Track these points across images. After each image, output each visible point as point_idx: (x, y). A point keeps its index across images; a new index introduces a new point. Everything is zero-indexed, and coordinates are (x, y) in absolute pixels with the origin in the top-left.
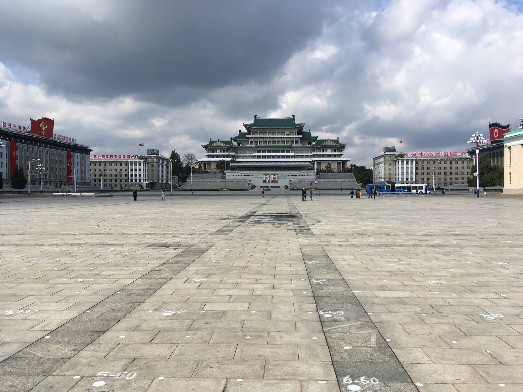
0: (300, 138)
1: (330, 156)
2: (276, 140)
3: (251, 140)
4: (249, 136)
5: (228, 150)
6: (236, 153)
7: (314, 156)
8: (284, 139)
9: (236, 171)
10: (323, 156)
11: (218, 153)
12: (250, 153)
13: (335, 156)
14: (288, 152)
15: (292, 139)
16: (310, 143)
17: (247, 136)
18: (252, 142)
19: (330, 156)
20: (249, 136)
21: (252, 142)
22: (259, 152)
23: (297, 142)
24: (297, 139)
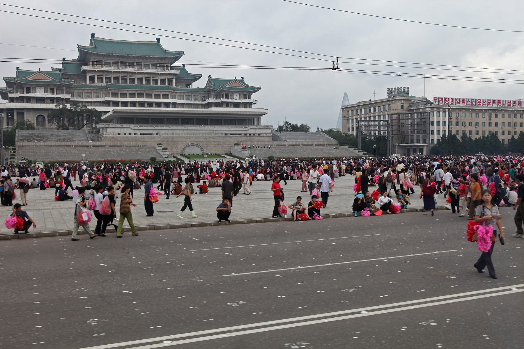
0: (176, 75)
1: (236, 105)
2: (136, 76)
3: (92, 75)
4: (88, 68)
5: (60, 88)
6: (73, 96)
7: (209, 105)
8: (148, 76)
9: (125, 126)
10: (227, 105)
11: (40, 93)
12: (97, 97)
13: (245, 105)
14: (166, 96)
15: (163, 77)
16: (188, 85)
17: (84, 68)
18: (92, 79)
19: (236, 105)
20: (88, 68)
21: (92, 79)
22: (115, 95)
23: (170, 82)
24: (171, 77)
